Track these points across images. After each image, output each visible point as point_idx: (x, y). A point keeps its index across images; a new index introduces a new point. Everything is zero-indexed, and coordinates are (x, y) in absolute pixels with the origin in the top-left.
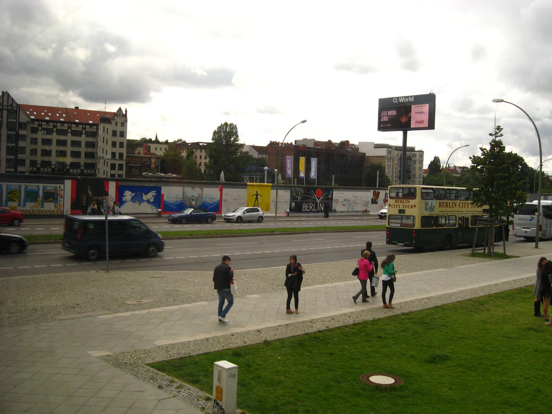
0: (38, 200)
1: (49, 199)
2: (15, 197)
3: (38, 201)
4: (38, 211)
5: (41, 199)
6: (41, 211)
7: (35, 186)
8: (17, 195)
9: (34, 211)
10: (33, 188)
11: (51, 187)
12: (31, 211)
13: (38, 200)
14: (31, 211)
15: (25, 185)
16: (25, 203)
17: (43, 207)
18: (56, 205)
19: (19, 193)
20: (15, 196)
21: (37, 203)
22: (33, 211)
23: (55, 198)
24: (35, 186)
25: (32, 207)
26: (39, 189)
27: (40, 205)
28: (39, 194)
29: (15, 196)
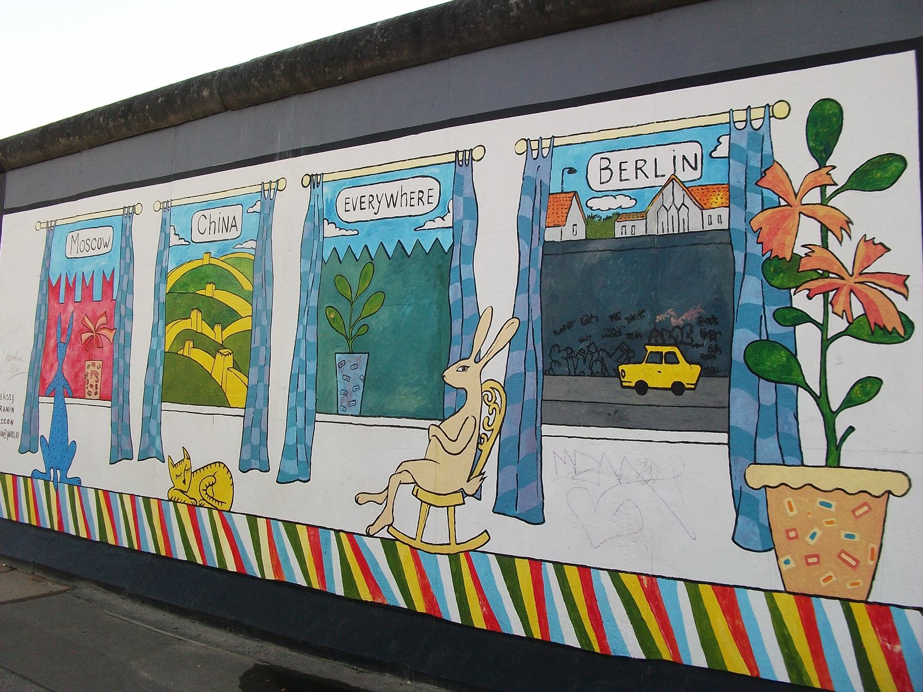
0: (452, 376)
1: (633, 373)
2: (213, 349)
3: (462, 393)
4: (454, 558)
5: (497, 369)
6: (507, 562)
7: (419, 172)
8: (232, 315)
9: (404, 552)
10: (392, 201)
11: (665, 139)
12: (375, 549)
13: (452, 376)
14: (375, 549)
15: (314, 181)
16: (309, 420)
17: (535, 517)
18: (757, 476)
19: (249, 298)
20: (217, 335)
21: (451, 425)
22: (389, 546)
23: (742, 337)
24: (419, 172)
25: (385, 498)
26: (472, 208)
27: (491, 469)
28: (470, 287)
29: (217, 335)
